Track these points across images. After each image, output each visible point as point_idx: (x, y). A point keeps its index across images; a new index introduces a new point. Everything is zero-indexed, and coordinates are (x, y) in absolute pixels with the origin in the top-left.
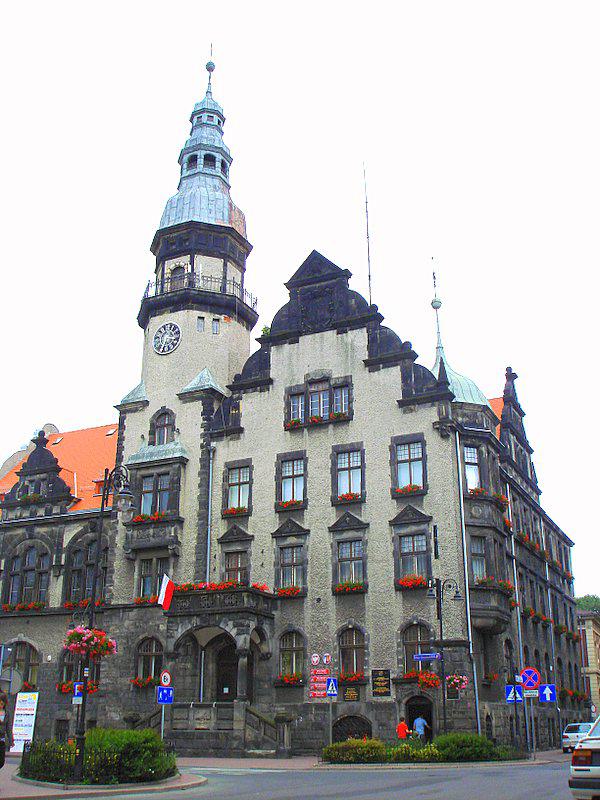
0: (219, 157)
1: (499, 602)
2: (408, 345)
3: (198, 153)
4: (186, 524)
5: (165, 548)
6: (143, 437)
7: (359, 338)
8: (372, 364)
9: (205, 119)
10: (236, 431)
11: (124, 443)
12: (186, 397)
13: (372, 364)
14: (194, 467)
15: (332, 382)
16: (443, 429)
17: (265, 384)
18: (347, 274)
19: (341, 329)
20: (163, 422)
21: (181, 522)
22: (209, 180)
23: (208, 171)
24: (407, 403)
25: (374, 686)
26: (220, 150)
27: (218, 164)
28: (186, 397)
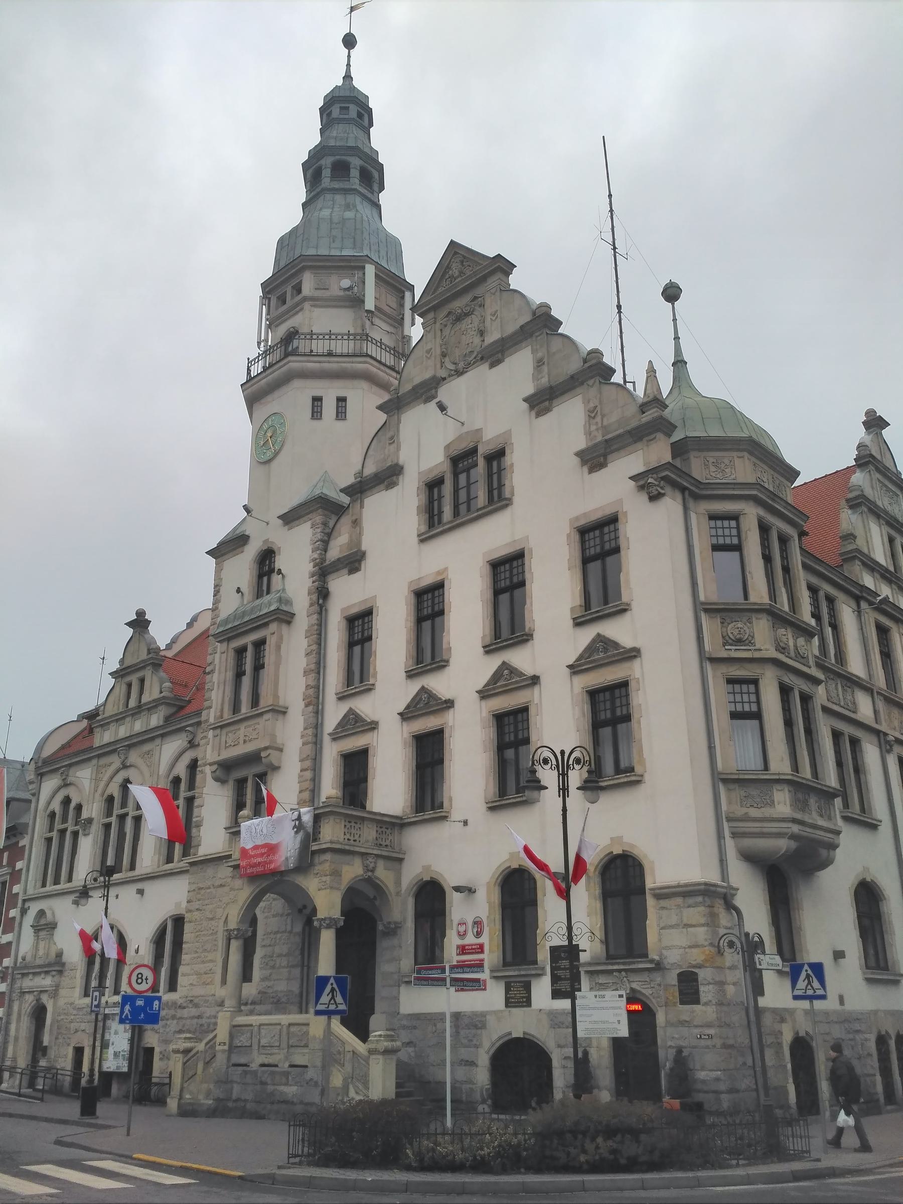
0: (355, 162)
1: (800, 804)
2: (596, 353)
3: (323, 162)
4: (291, 712)
5: (254, 758)
6: (239, 590)
7: (520, 372)
8: (541, 401)
9: (336, 112)
10: (353, 562)
11: (220, 605)
12: (290, 518)
13: (541, 401)
14: (303, 621)
15: (481, 450)
16: (651, 485)
17: (389, 476)
18: (502, 266)
19: (494, 358)
20: (266, 562)
21: (281, 712)
22: (339, 198)
23: (336, 185)
24: (594, 458)
25: (555, 979)
26: (356, 151)
27: (355, 173)
28: (290, 518)
